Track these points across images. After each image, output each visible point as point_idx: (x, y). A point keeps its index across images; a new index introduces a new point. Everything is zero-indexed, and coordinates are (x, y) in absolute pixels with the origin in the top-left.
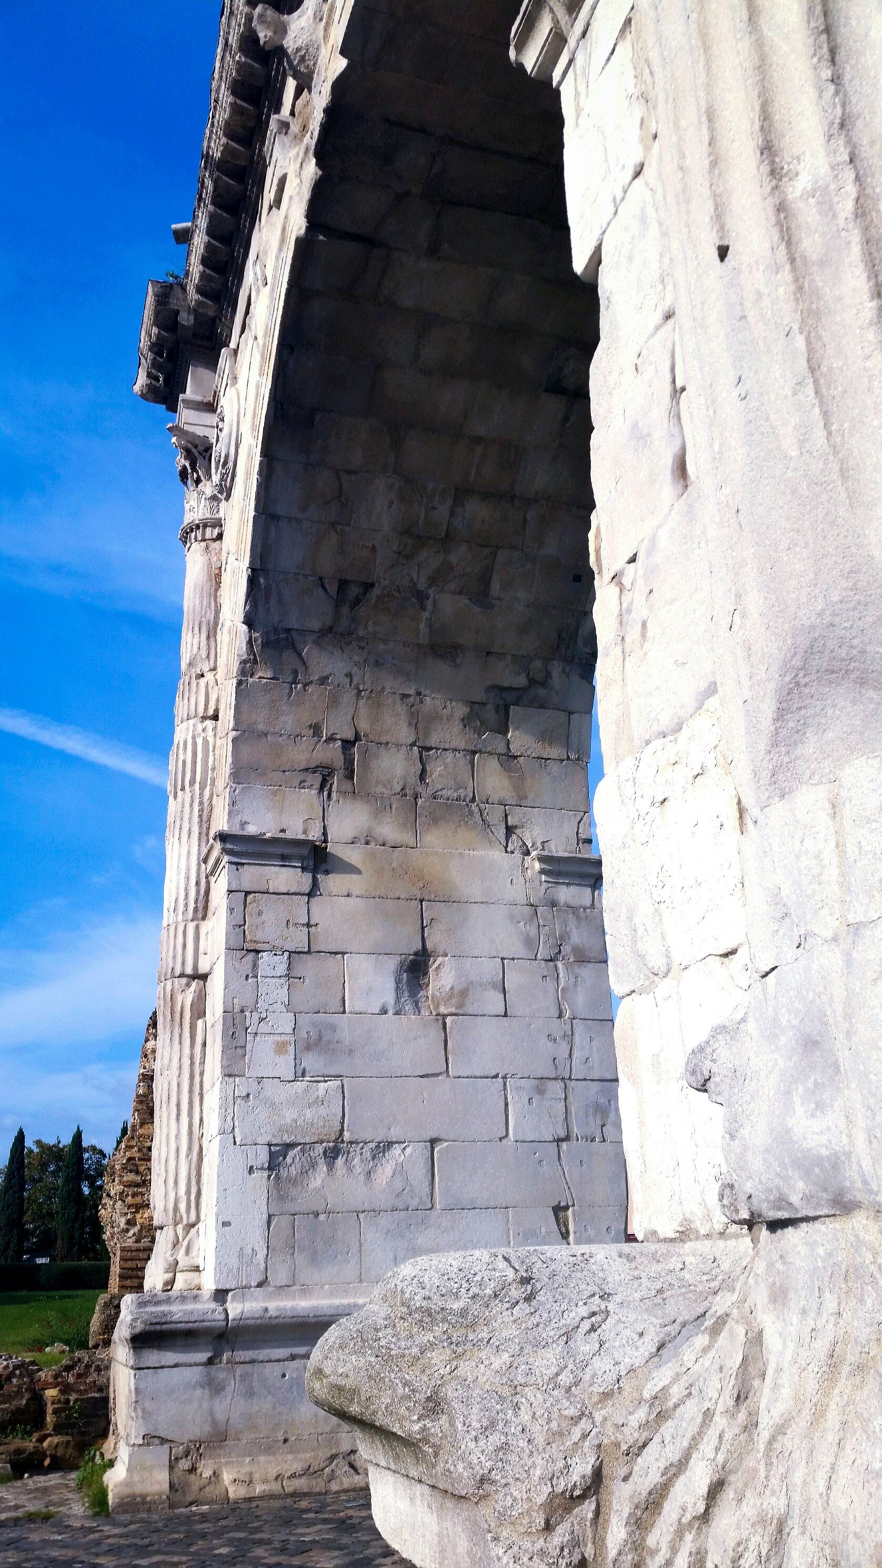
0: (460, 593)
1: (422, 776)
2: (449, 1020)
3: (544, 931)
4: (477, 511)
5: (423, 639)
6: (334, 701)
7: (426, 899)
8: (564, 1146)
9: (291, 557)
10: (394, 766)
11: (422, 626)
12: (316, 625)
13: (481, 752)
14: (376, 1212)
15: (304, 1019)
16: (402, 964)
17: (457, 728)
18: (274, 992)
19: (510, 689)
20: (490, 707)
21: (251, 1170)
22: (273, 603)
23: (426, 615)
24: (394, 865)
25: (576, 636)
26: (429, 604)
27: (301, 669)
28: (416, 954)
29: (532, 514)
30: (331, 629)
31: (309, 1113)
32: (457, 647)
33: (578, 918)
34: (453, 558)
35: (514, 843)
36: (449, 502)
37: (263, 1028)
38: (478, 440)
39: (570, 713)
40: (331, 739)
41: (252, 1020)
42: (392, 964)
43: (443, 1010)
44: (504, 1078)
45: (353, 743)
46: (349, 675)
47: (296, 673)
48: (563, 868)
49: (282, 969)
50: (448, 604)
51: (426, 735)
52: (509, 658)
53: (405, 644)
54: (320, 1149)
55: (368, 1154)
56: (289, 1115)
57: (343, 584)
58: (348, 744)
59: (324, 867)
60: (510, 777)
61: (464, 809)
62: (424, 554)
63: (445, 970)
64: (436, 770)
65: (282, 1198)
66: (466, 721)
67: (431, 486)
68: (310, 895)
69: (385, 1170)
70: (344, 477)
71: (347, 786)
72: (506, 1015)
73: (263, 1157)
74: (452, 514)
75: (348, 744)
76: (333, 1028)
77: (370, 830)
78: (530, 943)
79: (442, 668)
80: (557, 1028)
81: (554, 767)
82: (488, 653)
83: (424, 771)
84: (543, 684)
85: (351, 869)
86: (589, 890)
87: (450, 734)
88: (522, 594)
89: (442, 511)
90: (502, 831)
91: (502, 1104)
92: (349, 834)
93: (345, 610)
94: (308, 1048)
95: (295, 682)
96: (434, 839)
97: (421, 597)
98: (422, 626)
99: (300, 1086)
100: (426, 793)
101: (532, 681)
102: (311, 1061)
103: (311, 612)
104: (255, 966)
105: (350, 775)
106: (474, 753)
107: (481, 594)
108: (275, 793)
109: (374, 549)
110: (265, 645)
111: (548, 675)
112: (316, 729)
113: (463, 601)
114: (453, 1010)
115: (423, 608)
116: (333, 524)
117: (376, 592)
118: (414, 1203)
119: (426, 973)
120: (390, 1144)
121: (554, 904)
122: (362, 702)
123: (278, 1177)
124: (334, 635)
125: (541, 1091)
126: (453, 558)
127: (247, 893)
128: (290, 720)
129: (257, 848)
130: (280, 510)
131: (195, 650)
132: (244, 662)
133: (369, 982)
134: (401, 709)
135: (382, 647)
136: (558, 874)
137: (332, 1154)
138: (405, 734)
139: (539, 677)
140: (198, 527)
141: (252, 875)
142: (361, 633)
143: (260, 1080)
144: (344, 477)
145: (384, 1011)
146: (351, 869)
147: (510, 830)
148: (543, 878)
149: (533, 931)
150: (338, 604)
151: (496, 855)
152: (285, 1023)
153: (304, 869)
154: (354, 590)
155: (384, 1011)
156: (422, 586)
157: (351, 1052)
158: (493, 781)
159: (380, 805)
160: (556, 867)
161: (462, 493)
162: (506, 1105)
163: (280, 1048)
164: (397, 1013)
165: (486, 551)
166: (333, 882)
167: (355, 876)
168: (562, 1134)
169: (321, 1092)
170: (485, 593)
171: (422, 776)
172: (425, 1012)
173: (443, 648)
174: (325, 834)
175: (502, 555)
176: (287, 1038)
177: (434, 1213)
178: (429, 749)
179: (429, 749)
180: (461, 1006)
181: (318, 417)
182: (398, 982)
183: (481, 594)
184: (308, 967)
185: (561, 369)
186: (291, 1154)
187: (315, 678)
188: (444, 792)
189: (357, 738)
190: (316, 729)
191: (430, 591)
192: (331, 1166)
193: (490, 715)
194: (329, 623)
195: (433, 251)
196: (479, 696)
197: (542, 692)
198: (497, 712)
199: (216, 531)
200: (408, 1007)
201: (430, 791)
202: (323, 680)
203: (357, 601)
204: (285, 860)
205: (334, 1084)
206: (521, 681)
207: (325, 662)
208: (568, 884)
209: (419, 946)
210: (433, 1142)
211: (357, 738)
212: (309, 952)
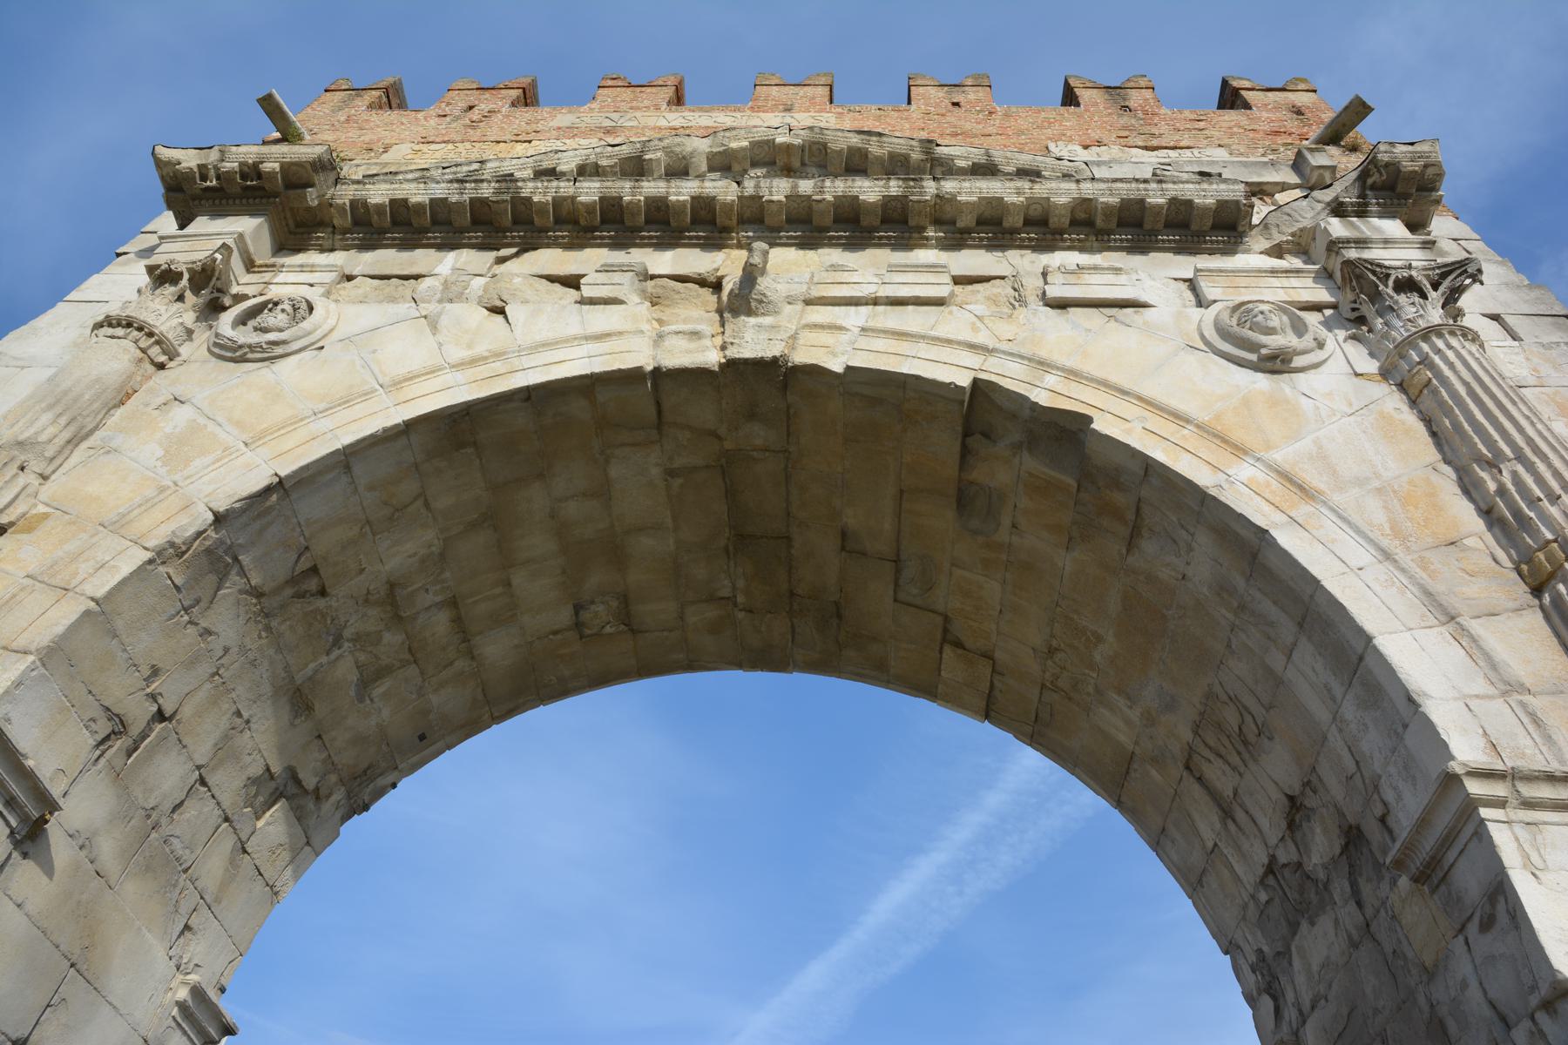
5: (299, 678)
11: (312, 666)
17: (239, 782)
20: (273, 785)
23: (324, 659)
26: (336, 653)
29: (461, 664)
32: (309, 708)
34: (388, 637)
36: (439, 599)
38: (508, 584)
46: (226, 650)
47: (198, 601)
50: (345, 669)
52: (325, 755)
57: (314, 570)
58: (160, 716)
60: (227, 870)
64: (190, 811)
67: (447, 574)
70: (419, 503)
71: (118, 763)
75: (160, 716)
82: (319, 737)
88: (386, 713)
89: (430, 598)
93: (289, 591)
96: (132, 890)
97: (337, 641)
98: (312, 666)
106: (226, 819)
107: (366, 683)
112: (155, 672)
117: (321, 603)
126: (388, 637)
128: (147, 644)
130: (358, 469)
131: (43, 438)
138: (202, 751)
140: (150, 335)
144: (419, 503)
146: (48, 869)
150: (292, 581)
154: (312, 584)
156: (347, 633)
165: (408, 656)
175: (412, 670)
181: (470, 450)
183: (366, 683)
185: (593, 602)
187: (204, 624)
194: (266, 589)
195: (671, 473)
196: (276, 769)
199: (163, 358)
203: (300, 595)
207: (228, 619)
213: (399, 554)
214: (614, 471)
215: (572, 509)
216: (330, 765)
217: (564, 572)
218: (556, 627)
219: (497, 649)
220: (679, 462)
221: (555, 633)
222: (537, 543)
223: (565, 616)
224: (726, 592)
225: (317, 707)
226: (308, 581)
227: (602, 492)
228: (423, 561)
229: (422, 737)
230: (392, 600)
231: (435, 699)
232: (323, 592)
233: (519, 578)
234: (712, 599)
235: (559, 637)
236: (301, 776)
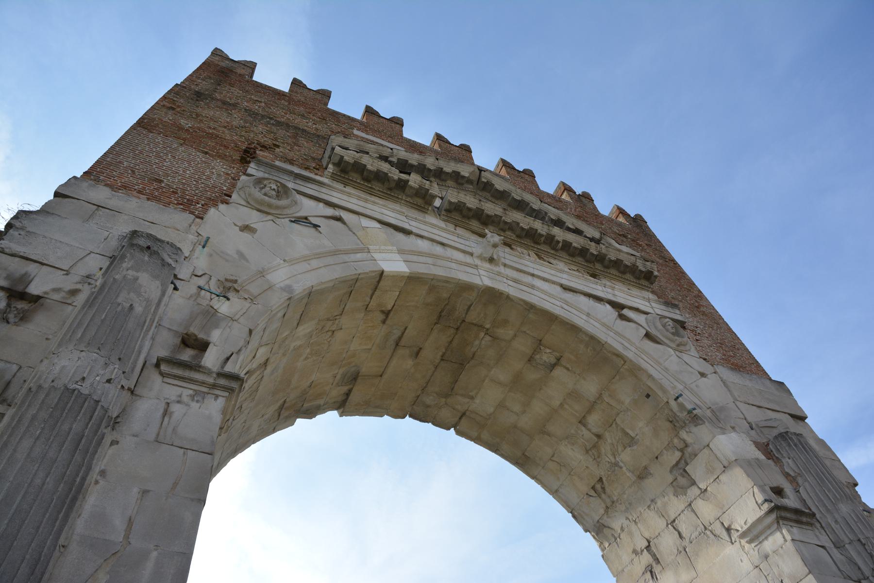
0: (625, 448)
3: (769, 578)
4: (593, 420)
5: (634, 478)
6: (631, 534)
10: (667, 543)
12: (602, 511)
19: (678, 463)
20: (680, 478)
22: (585, 517)
23: (624, 469)
26: (621, 464)
29: (606, 399)
30: (607, 507)
32: (646, 468)
34: (609, 441)
36: (583, 428)
38: (561, 405)
39: (708, 445)
40: (642, 551)
48: (755, 532)
50: (626, 456)
53: (630, 487)
57: (593, 488)
66: (676, 495)
67: (573, 431)
74: (589, 430)
75: (648, 547)
79: (649, 482)
82: (657, 458)
84: (687, 446)
87: (675, 505)
88: (641, 424)
93: (603, 496)
95: (616, 539)
97: (616, 464)
101: (681, 451)
103: (596, 507)
105: (657, 561)
106: (690, 505)
107: (631, 441)
109: (587, 467)
110: (597, 534)
111: (684, 441)
112: (635, 552)
115: (621, 468)
117: (604, 479)
121: (766, 557)
130: (555, 488)
135: (625, 496)
139: (682, 445)
142: (615, 499)
147: (728, 530)
148: (753, 545)
150: (599, 496)
154: (598, 486)
156: (613, 460)
161: (582, 422)
165: (614, 425)
170: (633, 438)
173: (643, 475)
175: (618, 421)
178: (674, 521)
179: (674, 521)
183: (631, 441)
187: (619, 531)
189: (649, 542)
193: (682, 481)
195: (472, 398)
196: (670, 478)
197: (689, 449)
198: (683, 477)
201: (687, 540)
202: (622, 529)
203: (603, 488)
206: (678, 454)
208: (766, 538)
211: (649, 542)
213: (574, 455)
214: (492, 410)
215: (517, 408)
216: (670, 446)
217: (540, 389)
218: (565, 371)
219: (590, 387)
220: (467, 400)
221: (568, 369)
222: (538, 408)
223: (558, 372)
224: (488, 338)
225: (644, 465)
226: (599, 488)
227: (501, 405)
228: (573, 444)
229: (648, 396)
230: (593, 449)
231: (627, 401)
232: (600, 480)
233: (556, 403)
234: (495, 338)
235: (568, 366)
236: (674, 462)
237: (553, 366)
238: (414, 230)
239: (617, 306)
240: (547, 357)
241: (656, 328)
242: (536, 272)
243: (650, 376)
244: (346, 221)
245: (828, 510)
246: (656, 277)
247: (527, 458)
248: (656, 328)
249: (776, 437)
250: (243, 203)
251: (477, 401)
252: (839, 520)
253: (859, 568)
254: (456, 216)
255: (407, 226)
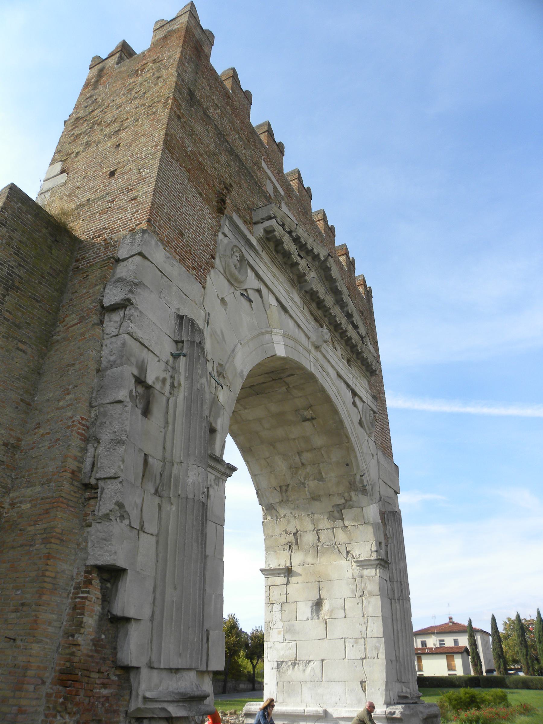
0: (314, 479)
1: (318, 539)
2: (327, 620)
3: (358, 587)
4: (307, 456)
5: (309, 496)
6: (288, 522)
7: (320, 582)
8: (364, 661)
9: (264, 484)
10: (309, 538)
11: (307, 493)
12: (278, 501)
13: (335, 527)
14: (306, 682)
15: (285, 623)
16: (313, 604)
17: (326, 521)
18: (277, 615)
20: (336, 512)
21: (272, 669)
22: (265, 498)
23: (307, 489)
24: (311, 571)
25: (355, 482)
26: (306, 485)
27: (278, 515)
28: (317, 600)
30: (282, 501)
31: (287, 652)
32: (319, 496)
33: (370, 580)
34: (308, 470)
35: (350, 556)
36: (297, 456)
37: (275, 627)
38: (294, 439)
39: (362, 507)
40: (290, 533)
41: (272, 625)
42: (310, 604)
43: (326, 618)
44: (345, 639)
45: (297, 533)
46: (291, 513)
47: (276, 515)
48: (363, 564)
49: (279, 609)
50: (312, 484)
51: (317, 526)
52: (336, 495)
53: (304, 499)
54: (290, 663)
55: (304, 664)
56: (282, 653)
57: (281, 487)
58: (295, 534)
59: (291, 575)
60: (346, 534)
61: (335, 547)
62: (300, 472)
63: (327, 604)
64: (322, 537)
65: (280, 677)
66: (328, 519)
67: (290, 454)
68: (287, 584)
69: (309, 670)
70: (267, 460)
71: (297, 547)
72: (345, 617)
73: (275, 665)
74: (300, 459)
75: (295, 534)
76: (293, 626)
77: (304, 560)
78: (353, 591)
79: (317, 504)
80: (362, 620)
81: (360, 527)
83: (319, 538)
84: (351, 500)
85: (299, 575)
86: (374, 570)
87: (325, 523)
88: (333, 475)
89: (297, 459)
90: (345, 553)
91: (344, 647)
92: (298, 563)
93: (284, 494)
94: (287, 632)
95: (277, 518)
96: (323, 560)
97: (303, 484)
99: (284, 644)
100: (320, 544)
101: (346, 501)
102: (288, 637)
103: (275, 498)
104: (272, 608)
105: (297, 543)
107: (321, 479)
108: (277, 554)
109: (284, 475)
110: (266, 510)
111: (351, 497)
112: (286, 531)
113: (316, 482)
114: (328, 617)
115: (305, 487)
116: (271, 472)
117: (290, 486)
118: (316, 680)
119: (322, 606)
120: (310, 661)
121: (362, 577)
122: (296, 520)
123: (279, 671)
124: (284, 502)
125: (356, 643)
126: (308, 470)
127: (270, 586)
128: (278, 530)
129: (270, 572)
130: (256, 473)
132: (264, 516)
133: (304, 610)
134: (308, 519)
135: (297, 502)
136: (363, 566)
137: (294, 664)
138: (311, 527)
139: (348, 498)
141: (272, 580)
142: (290, 499)
143: (274, 642)
145: (308, 619)
146: (299, 575)
147: (348, 552)
148: (358, 568)
149: (354, 587)
150: (281, 493)
151: (343, 562)
152: (280, 624)
153: (285, 576)
154: (284, 488)
155: (308, 619)
156: (303, 481)
157: (298, 633)
158: (341, 536)
159: (307, 552)
160: (361, 564)
161: (299, 453)
162: (345, 648)
163: (279, 633)
164: (312, 620)
165: (316, 465)
166: (293, 580)
167: (299, 577)
168: (363, 657)
169: (290, 646)
170: (322, 477)
171: (318, 539)
172: (321, 618)
173: (315, 498)
174: (291, 564)
175: (321, 465)
176: (280, 630)
177: (323, 683)
178: (319, 530)
179: (319, 530)
180: (331, 616)
182: (312, 610)
183: (321, 479)
184: (286, 607)
186: (283, 664)
188: (326, 544)
189: (297, 531)
190: (286, 531)
191: (306, 482)
192: (293, 668)
193: (336, 514)
194: (281, 499)
195: (245, 408)
196: (331, 509)
197: (351, 503)
198: (338, 513)
200: (315, 617)
201: (321, 544)
202: (284, 516)
203: (286, 490)
204: (279, 574)
205: (294, 643)
206: (343, 501)
207: (282, 511)
208: (367, 569)
209: (318, 597)
210: (323, 660)
211: (297, 531)
212: (286, 602)
216: (341, 495)
219: (319, 441)
222: (280, 432)
223: (307, 424)
225: (319, 494)
226: (283, 489)
230: (294, 469)
231: (334, 459)
232: (288, 486)
233: (292, 436)
235: (315, 425)
237: (306, 420)
238: (291, 312)
239: (354, 394)
240: (308, 414)
241: (365, 416)
242: (331, 361)
243: (356, 457)
244: (263, 295)
245: (395, 562)
246: (376, 374)
247: (250, 450)
248: (365, 416)
249: (390, 512)
250: (222, 271)
251: (246, 411)
252: (398, 569)
253: (394, 594)
254: (308, 296)
255: (289, 308)
